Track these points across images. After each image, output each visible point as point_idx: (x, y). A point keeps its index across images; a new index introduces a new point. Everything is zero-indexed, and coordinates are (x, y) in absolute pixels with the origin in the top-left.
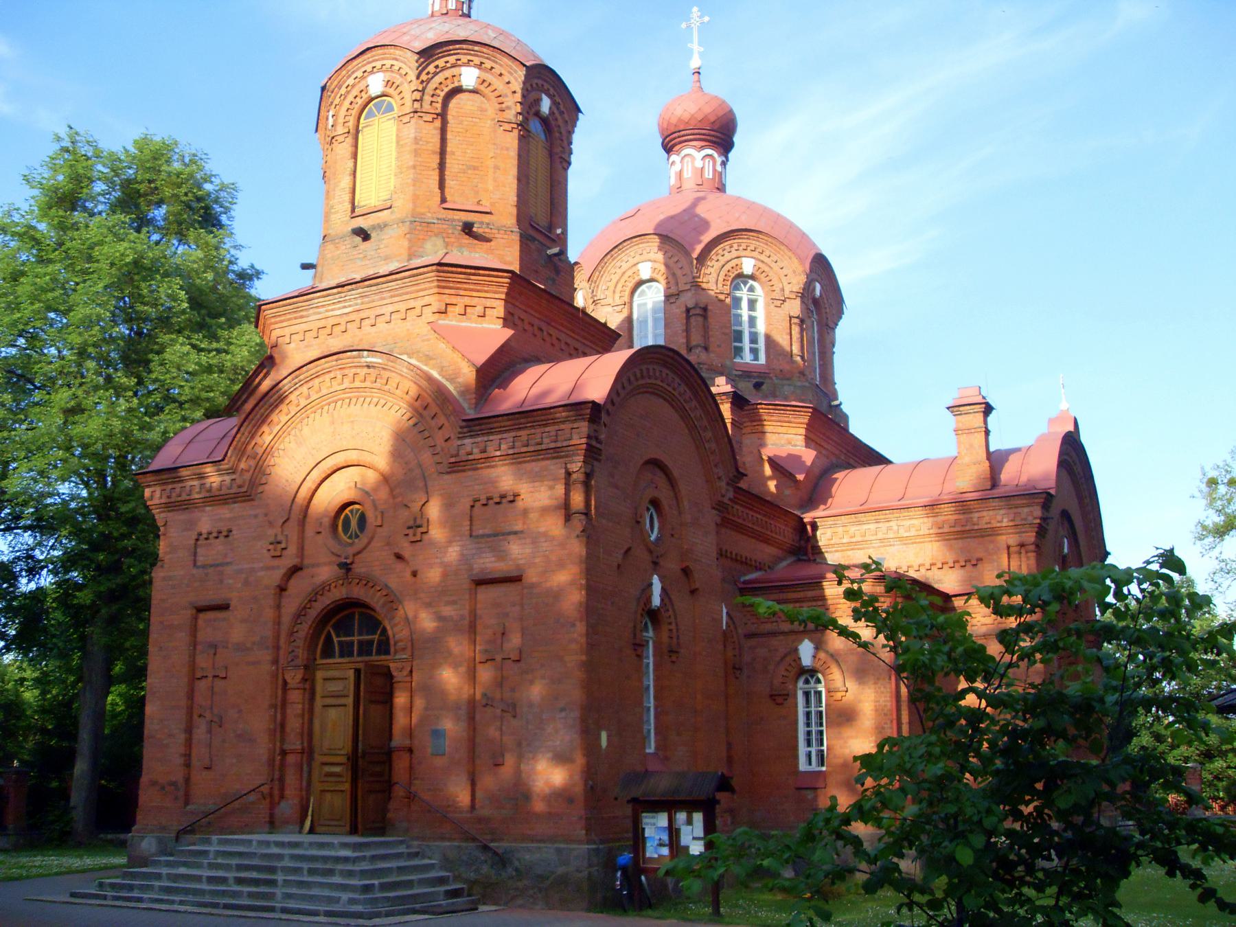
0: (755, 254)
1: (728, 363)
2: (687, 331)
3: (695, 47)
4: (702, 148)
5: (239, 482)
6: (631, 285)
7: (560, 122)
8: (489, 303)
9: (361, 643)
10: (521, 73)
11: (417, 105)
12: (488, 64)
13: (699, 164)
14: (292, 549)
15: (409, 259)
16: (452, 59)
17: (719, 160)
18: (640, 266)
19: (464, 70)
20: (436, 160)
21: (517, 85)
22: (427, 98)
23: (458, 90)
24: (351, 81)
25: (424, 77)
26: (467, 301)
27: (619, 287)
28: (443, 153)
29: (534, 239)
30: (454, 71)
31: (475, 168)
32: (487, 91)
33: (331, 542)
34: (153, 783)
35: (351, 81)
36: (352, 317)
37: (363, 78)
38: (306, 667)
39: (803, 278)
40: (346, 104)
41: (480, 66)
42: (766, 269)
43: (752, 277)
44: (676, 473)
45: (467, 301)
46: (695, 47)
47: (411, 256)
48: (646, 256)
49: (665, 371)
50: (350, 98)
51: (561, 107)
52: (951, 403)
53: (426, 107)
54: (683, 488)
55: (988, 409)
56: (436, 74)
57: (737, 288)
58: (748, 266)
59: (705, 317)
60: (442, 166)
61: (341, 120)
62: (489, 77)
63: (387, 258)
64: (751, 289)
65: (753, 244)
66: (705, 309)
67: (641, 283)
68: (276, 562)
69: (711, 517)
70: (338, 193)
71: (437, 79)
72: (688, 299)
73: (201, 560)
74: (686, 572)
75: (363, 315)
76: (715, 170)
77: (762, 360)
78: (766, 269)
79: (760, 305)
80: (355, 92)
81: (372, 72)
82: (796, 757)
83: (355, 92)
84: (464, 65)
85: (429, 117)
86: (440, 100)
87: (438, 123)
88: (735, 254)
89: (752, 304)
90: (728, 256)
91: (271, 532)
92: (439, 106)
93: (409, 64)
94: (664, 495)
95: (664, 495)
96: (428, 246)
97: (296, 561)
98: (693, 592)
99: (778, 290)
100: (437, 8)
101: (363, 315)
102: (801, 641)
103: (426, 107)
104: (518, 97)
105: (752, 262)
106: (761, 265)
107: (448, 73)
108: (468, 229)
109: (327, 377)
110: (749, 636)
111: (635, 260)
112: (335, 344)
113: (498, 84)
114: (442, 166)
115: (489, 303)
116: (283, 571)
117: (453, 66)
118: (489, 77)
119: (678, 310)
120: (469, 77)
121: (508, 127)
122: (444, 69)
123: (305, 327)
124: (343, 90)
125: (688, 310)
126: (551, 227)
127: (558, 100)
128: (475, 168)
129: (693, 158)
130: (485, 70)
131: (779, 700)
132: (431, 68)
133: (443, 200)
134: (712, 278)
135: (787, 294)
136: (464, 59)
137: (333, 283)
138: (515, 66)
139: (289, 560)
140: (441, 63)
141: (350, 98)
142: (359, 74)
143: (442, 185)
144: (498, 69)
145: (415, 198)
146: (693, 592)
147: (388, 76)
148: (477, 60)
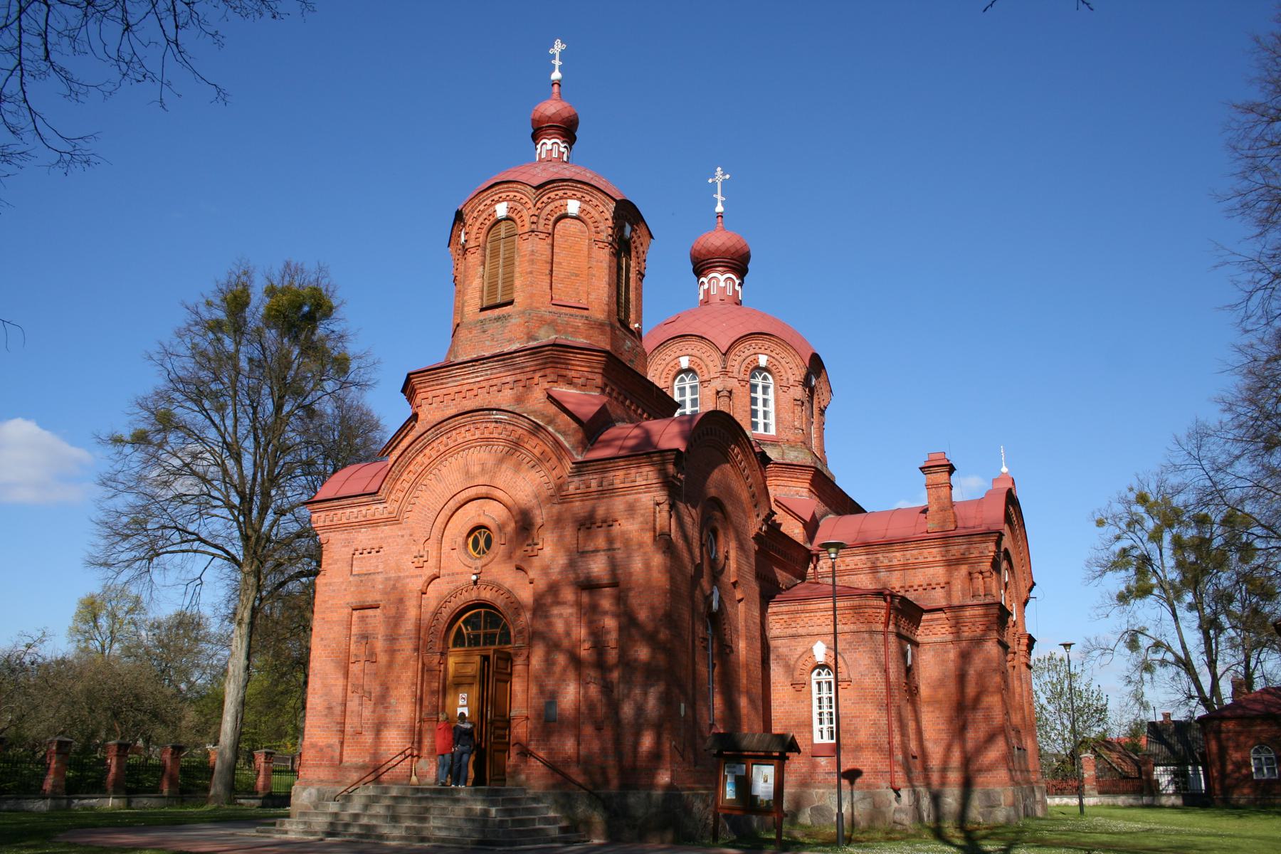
0: (768, 352)
3: (719, 197)
4: (724, 272)
5: (390, 509)
6: (672, 373)
9: (485, 635)
10: (612, 205)
11: (534, 226)
13: (722, 284)
14: (432, 562)
16: (560, 193)
17: (737, 282)
18: (681, 359)
19: (570, 202)
20: (548, 266)
21: (609, 215)
22: (542, 222)
23: (565, 216)
24: (481, 207)
25: (539, 205)
27: (664, 375)
30: (562, 202)
31: (577, 275)
32: (586, 218)
33: (464, 557)
34: (313, 746)
35: (481, 207)
36: (483, 384)
37: (491, 205)
38: (442, 654)
39: (804, 371)
40: (478, 224)
41: (579, 199)
43: (766, 369)
46: (719, 197)
50: (481, 220)
52: (923, 465)
55: (951, 469)
56: (548, 203)
57: (753, 377)
58: (763, 361)
61: (473, 237)
62: (585, 206)
63: (511, 341)
64: (765, 378)
65: (767, 344)
66: (730, 392)
68: (418, 571)
70: (470, 291)
71: (549, 207)
73: (356, 570)
75: (491, 382)
77: (772, 431)
79: (771, 391)
80: (484, 216)
81: (498, 202)
82: (811, 732)
83: (484, 216)
84: (570, 198)
86: (551, 223)
87: (549, 241)
88: (752, 351)
89: (765, 389)
91: (415, 549)
92: (550, 227)
97: (435, 571)
100: (543, 156)
101: (491, 382)
102: (815, 642)
103: (541, 228)
104: (610, 223)
107: (557, 203)
109: (463, 430)
111: (678, 353)
112: (470, 404)
116: (424, 578)
117: (561, 198)
118: (588, 208)
120: (573, 207)
121: (601, 245)
122: (554, 200)
123: (445, 391)
124: (475, 214)
125: (718, 393)
128: (577, 275)
129: (718, 281)
130: (586, 202)
131: (798, 687)
132: (545, 199)
134: (736, 370)
135: (791, 382)
136: (570, 193)
137: (466, 358)
138: (607, 200)
139: (429, 571)
140: (552, 195)
141: (481, 220)
142: (488, 202)
144: (595, 202)
145: (532, 296)
147: (511, 204)
148: (579, 195)
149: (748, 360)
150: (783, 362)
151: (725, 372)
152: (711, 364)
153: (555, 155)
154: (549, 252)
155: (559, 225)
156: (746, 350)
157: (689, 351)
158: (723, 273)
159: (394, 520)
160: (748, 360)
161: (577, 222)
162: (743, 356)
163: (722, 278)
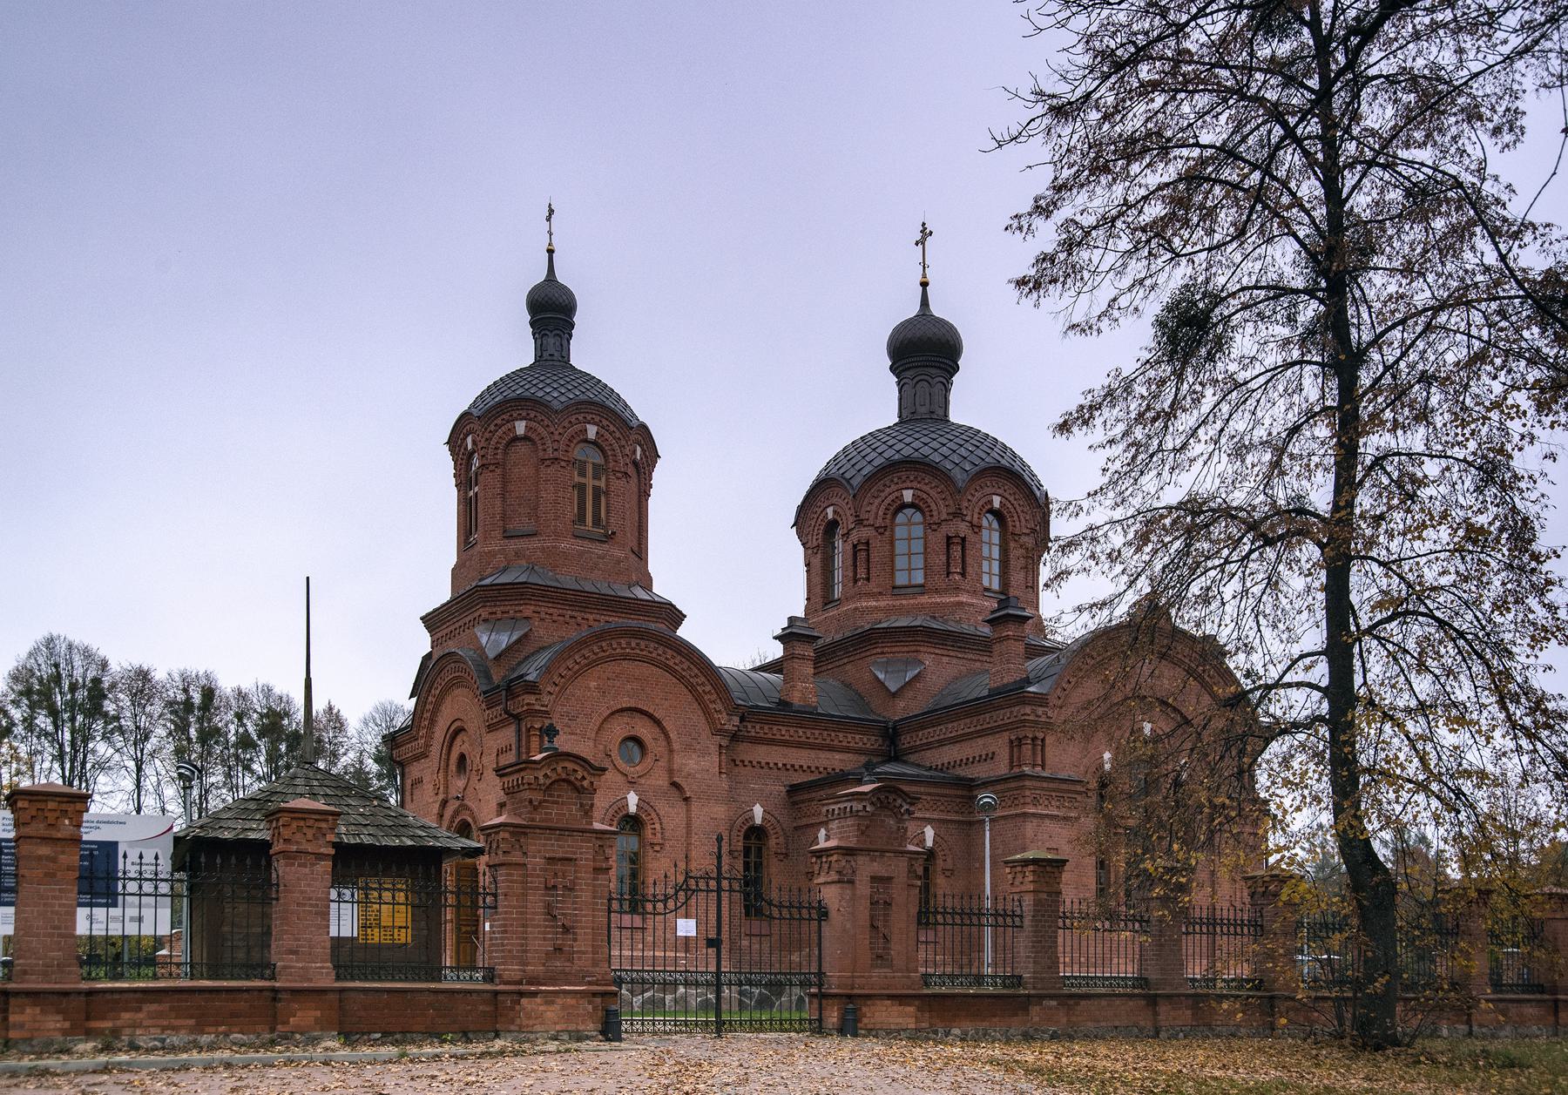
2: (855, 566)
48: (834, 500)
58: (908, 496)
66: (867, 543)
69: (711, 743)
72: (854, 538)
74: (674, 784)
88: (894, 487)
94: (645, 731)
95: (645, 731)
98: (686, 799)
105: (911, 492)
119: (849, 547)
125: (855, 546)
135: (944, 516)
146: (686, 799)
150: (932, 493)
151: (859, 522)
157: (834, 500)
159: (424, 755)
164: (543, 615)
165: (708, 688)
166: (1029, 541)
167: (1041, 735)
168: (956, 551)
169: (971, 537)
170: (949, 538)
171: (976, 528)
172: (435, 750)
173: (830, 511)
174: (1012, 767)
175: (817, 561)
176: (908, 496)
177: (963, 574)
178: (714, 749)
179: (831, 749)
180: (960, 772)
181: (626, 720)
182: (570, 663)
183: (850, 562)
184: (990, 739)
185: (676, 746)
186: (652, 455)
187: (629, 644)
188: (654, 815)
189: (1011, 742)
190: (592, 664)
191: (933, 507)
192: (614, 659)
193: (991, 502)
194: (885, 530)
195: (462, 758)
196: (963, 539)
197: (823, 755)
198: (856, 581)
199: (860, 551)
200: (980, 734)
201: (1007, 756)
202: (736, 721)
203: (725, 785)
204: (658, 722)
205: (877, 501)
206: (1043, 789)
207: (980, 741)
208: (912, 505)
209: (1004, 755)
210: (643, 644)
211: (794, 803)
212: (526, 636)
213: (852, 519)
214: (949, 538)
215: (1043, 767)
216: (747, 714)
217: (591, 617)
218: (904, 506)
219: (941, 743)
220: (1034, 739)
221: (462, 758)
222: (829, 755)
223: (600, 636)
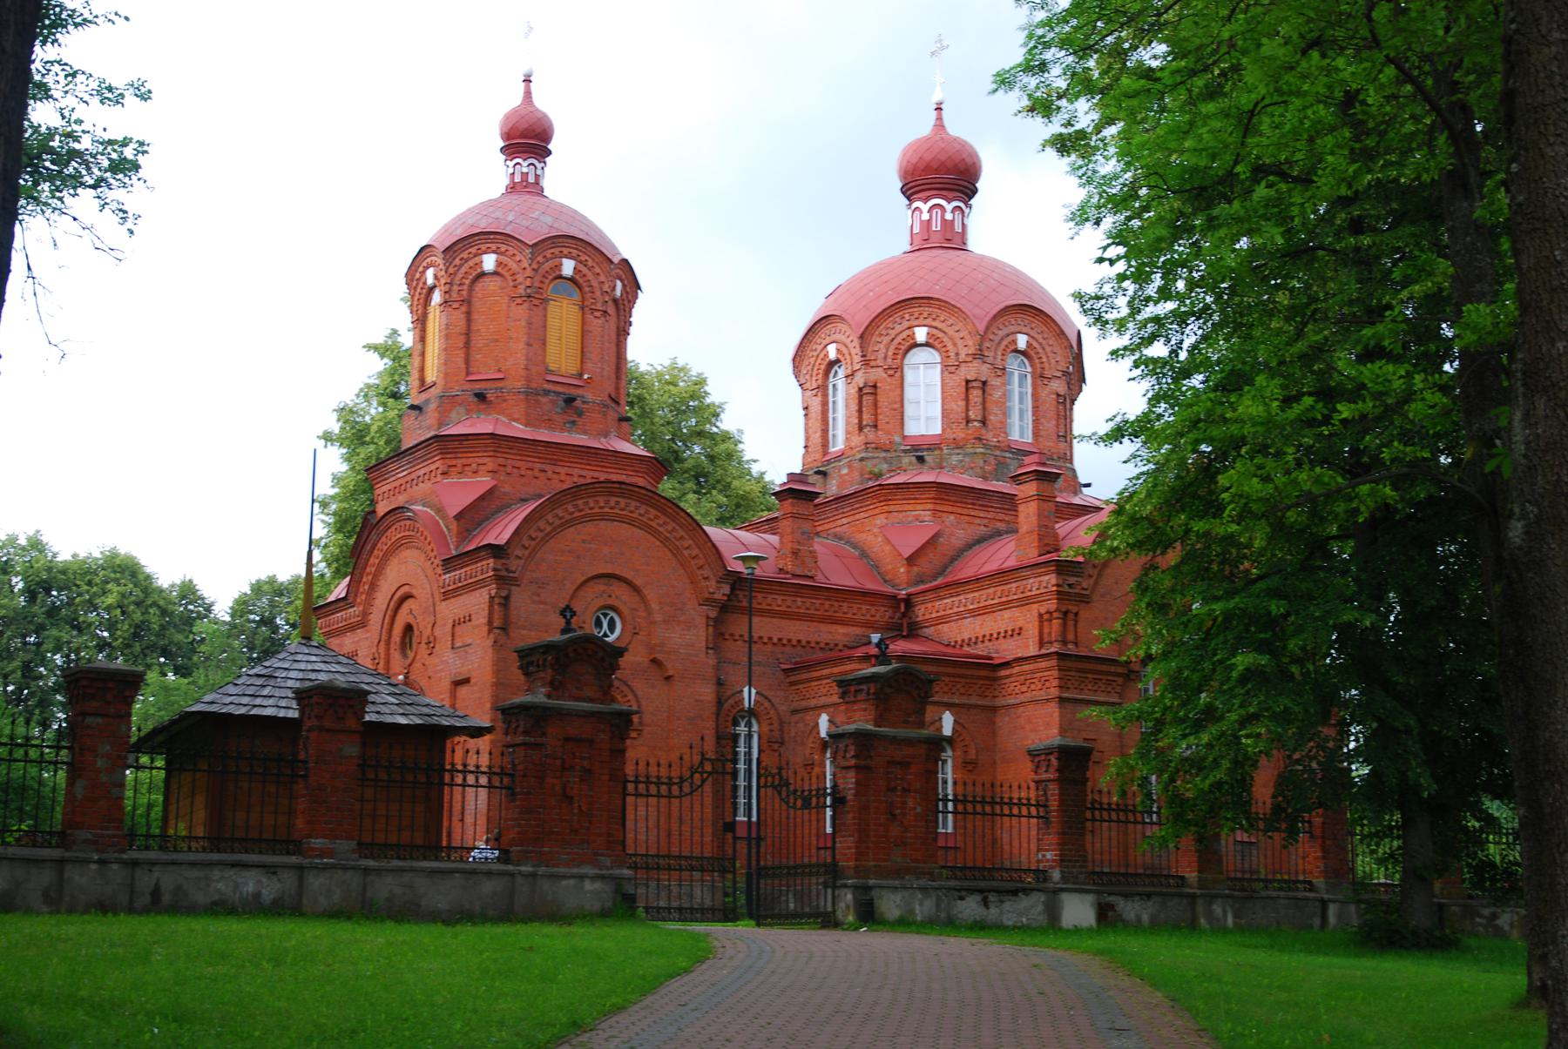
1: (897, 439)
2: (860, 411)
7: (590, 276)
8: (481, 461)
12: (503, 248)
13: (926, 216)
15: (441, 425)
16: (473, 250)
22: (455, 288)
23: (483, 274)
25: (451, 270)
26: (464, 461)
28: (468, 334)
29: (547, 392)
42: (941, 335)
44: (638, 582)
45: (464, 461)
47: (441, 425)
48: (834, 337)
49: (613, 500)
51: (590, 263)
53: (455, 295)
54: (650, 593)
58: (921, 334)
59: (875, 394)
60: (467, 345)
62: (504, 259)
65: (926, 310)
66: (875, 386)
67: (832, 364)
71: (463, 270)
72: (859, 379)
74: (655, 661)
76: (944, 220)
78: (941, 335)
85: (455, 305)
88: (906, 324)
90: (898, 328)
93: (439, 260)
96: (453, 415)
99: (952, 354)
106: (935, 331)
107: (471, 263)
108: (481, 397)
110: (795, 712)
113: (513, 266)
114: (467, 345)
115: (481, 461)
119: (854, 391)
120: (489, 262)
125: (860, 389)
126: (581, 375)
127: (583, 258)
132: (457, 261)
133: (468, 374)
134: (881, 355)
135: (962, 357)
136: (484, 247)
140: (464, 255)
143: (467, 361)
145: (446, 375)
146: (668, 678)
148: (494, 247)
149: (899, 339)
150: (950, 331)
151: (866, 363)
152: (853, 352)
153: (518, 179)
154: (462, 323)
155: (479, 286)
156: (897, 327)
157: (834, 337)
158: (926, 200)
159: (362, 624)
160: (899, 339)
161: (497, 278)
162: (893, 333)
163: (925, 207)
164: (509, 469)
165: (695, 551)
166: (1059, 386)
167: (1074, 609)
168: (976, 394)
169: (996, 382)
170: (968, 382)
171: (1002, 371)
172: (376, 618)
173: (832, 352)
174: (1041, 644)
175: (816, 403)
176: (921, 334)
177: (984, 422)
178: (701, 621)
179: (836, 622)
180: (980, 650)
181: (602, 587)
182: (541, 524)
183: (854, 407)
184: (1016, 612)
185: (658, 617)
186: (633, 286)
187: (607, 502)
188: (630, 697)
189: (1041, 615)
190: (567, 524)
191: (950, 347)
192: (591, 518)
193: (1014, 342)
194: (897, 372)
195: (409, 628)
196: (984, 383)
197: (824, 628)
198: (861, 429)
199: (867, 396)
200: (1005, 606)
201: (1036, 633)
202: (726, 589)
203: (712, 661)
204: (636, 589)
205: (886, 340)
206: (1079, 670)
207: (1007, 614)
208: (927, 345)
209: (1032, 631)
210: (623, 502)
211: (792, 684)
212: (490, 492)
213: (857, 358)
214: (968, 382)
215: (1076, 644)
216: (737, 582)
217: (562, 470)
218: (916, 345)
219: (960, 616)
220: (1066, 613)
221: (409, 628)
222: (833, 628)
223: (576, 492)
